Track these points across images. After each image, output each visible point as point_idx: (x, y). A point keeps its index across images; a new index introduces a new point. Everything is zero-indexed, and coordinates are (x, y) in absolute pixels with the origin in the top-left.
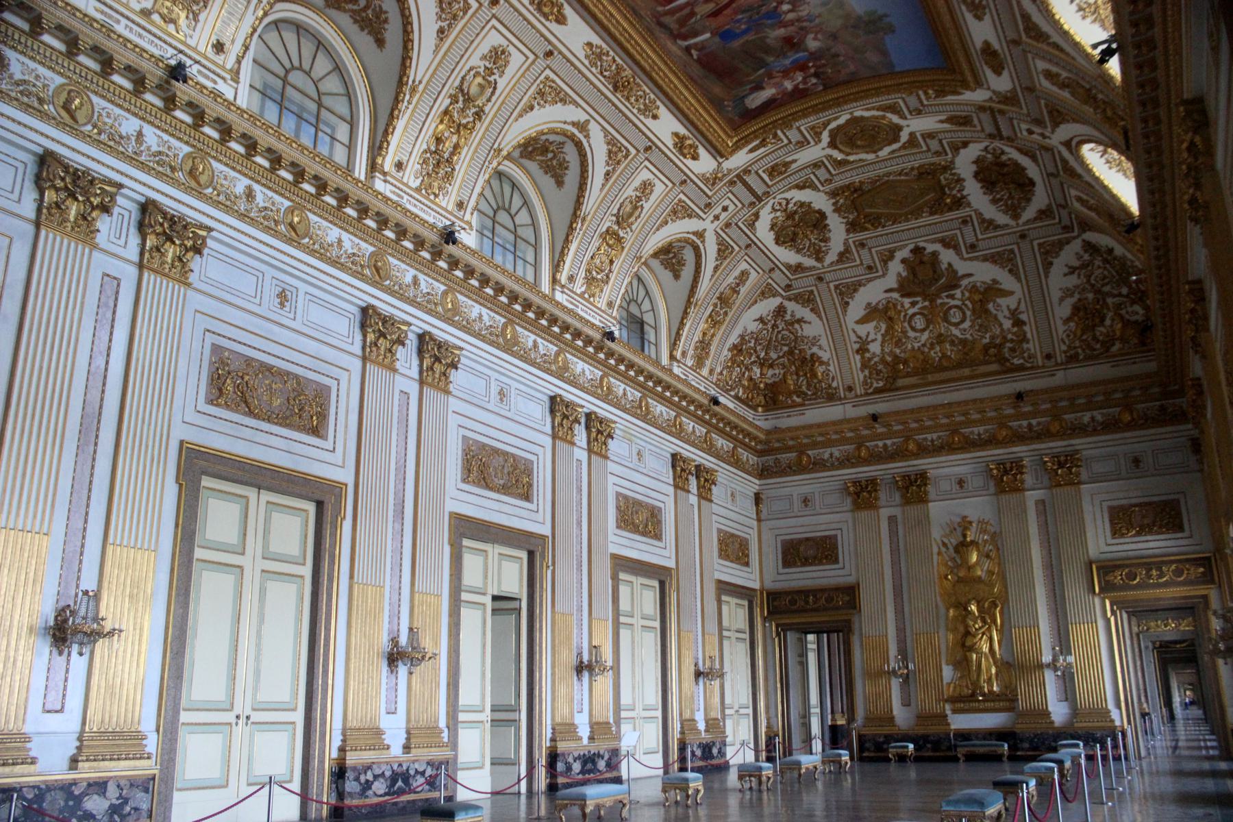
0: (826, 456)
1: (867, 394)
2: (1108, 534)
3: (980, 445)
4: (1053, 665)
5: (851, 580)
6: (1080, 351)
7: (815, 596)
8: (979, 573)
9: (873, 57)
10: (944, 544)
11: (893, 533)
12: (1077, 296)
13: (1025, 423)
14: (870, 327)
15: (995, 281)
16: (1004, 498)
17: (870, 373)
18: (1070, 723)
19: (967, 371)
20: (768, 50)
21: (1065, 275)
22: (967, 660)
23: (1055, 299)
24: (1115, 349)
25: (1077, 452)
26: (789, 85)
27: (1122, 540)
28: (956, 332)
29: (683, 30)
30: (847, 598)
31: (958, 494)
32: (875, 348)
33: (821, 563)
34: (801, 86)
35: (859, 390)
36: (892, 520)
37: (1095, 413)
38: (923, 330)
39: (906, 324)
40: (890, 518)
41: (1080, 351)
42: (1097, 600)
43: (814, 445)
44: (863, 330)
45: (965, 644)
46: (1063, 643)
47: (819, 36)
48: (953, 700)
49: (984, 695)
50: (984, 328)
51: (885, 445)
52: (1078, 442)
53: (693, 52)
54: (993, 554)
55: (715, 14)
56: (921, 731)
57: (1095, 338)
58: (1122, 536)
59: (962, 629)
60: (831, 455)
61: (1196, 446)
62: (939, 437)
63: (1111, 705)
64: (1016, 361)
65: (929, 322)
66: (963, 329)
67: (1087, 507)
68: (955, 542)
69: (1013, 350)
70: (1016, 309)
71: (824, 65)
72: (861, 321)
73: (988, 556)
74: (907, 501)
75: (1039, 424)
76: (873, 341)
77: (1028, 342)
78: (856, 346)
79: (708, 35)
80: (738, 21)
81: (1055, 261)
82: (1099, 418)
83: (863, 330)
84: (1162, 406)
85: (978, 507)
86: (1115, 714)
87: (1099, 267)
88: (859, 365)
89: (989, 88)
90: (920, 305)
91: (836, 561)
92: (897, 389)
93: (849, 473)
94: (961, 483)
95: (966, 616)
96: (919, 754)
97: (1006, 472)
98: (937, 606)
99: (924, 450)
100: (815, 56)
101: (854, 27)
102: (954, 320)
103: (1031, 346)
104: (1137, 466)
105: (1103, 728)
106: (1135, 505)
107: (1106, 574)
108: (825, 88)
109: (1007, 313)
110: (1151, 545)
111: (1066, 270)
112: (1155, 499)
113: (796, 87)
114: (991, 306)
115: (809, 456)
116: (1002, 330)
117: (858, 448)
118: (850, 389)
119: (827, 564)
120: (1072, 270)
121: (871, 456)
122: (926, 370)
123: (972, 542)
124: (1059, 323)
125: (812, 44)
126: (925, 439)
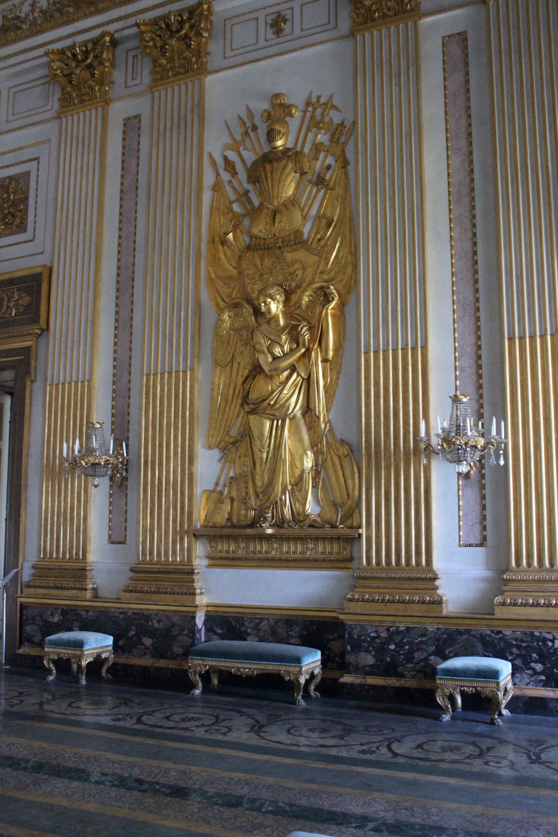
10: (229, 165)
11: (130, 152)
18: (484, 609)
30: (26, 300)
36: (132, 125)
48: (212, 534)
49: (280, 523)
68: (250, 157)
73: (320, 181)
74: (160, 77)
91: (22, 228)
93: (60, 36)
96: (123, 660)
98: (198, 306)
123: (287, 154)
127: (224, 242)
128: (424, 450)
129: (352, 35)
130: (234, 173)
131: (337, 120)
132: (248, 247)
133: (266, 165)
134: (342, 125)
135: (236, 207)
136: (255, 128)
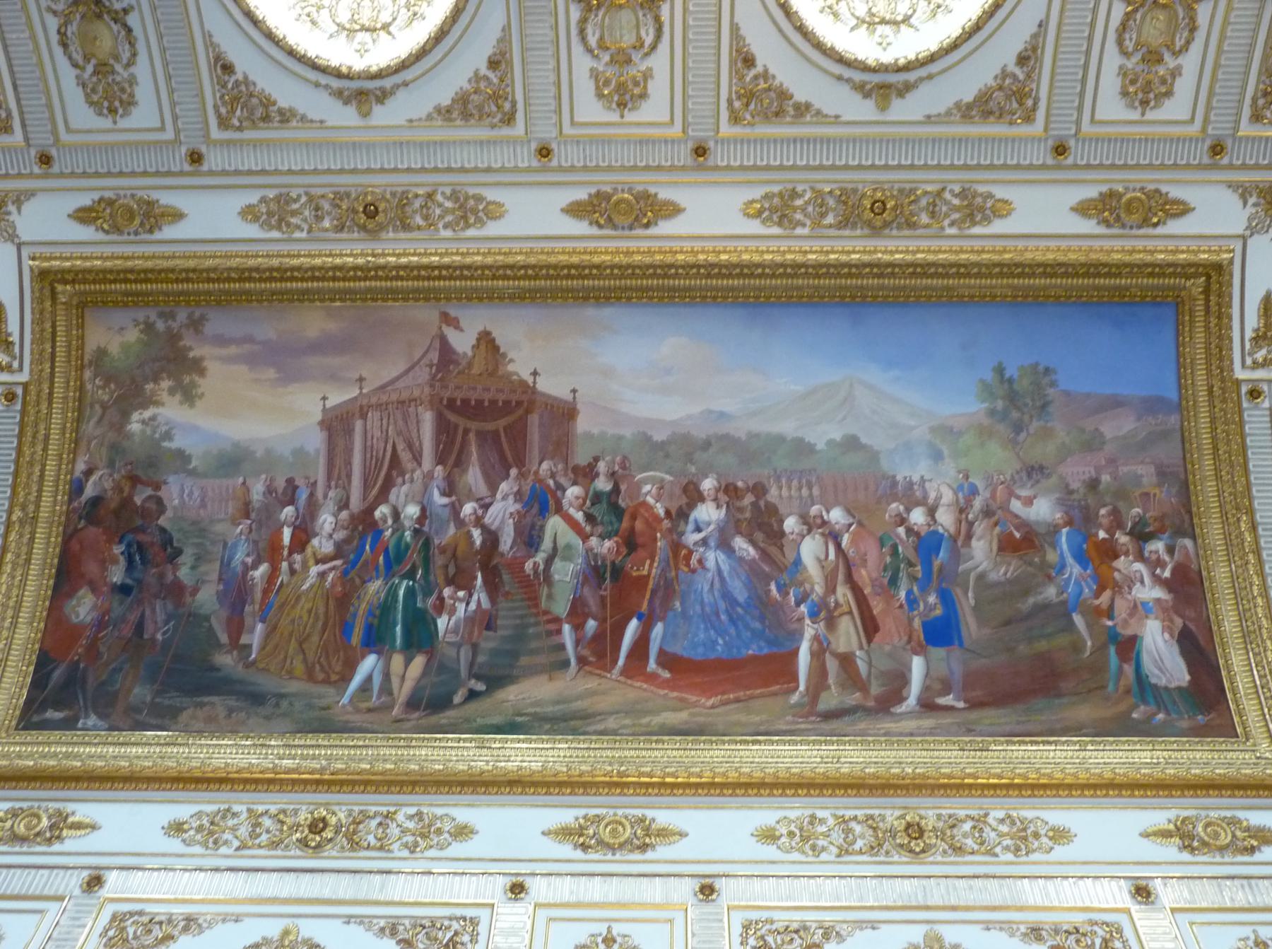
9: (1118, 427)
20: (1020, 587)
26: (1149, 592)
29: (875, 689)
34: (1167, 574)
47: (1024, 493)
53: (942, 701)
55: (870, 627)
71: (1115, 513)
79: (917, 666)
80: (912, 601)
89: (1244, 239)
100: (1080, 516)
101: (1018, 428)
108: (1194, 538)
113: (1158, 580)
125: (1043, 510)
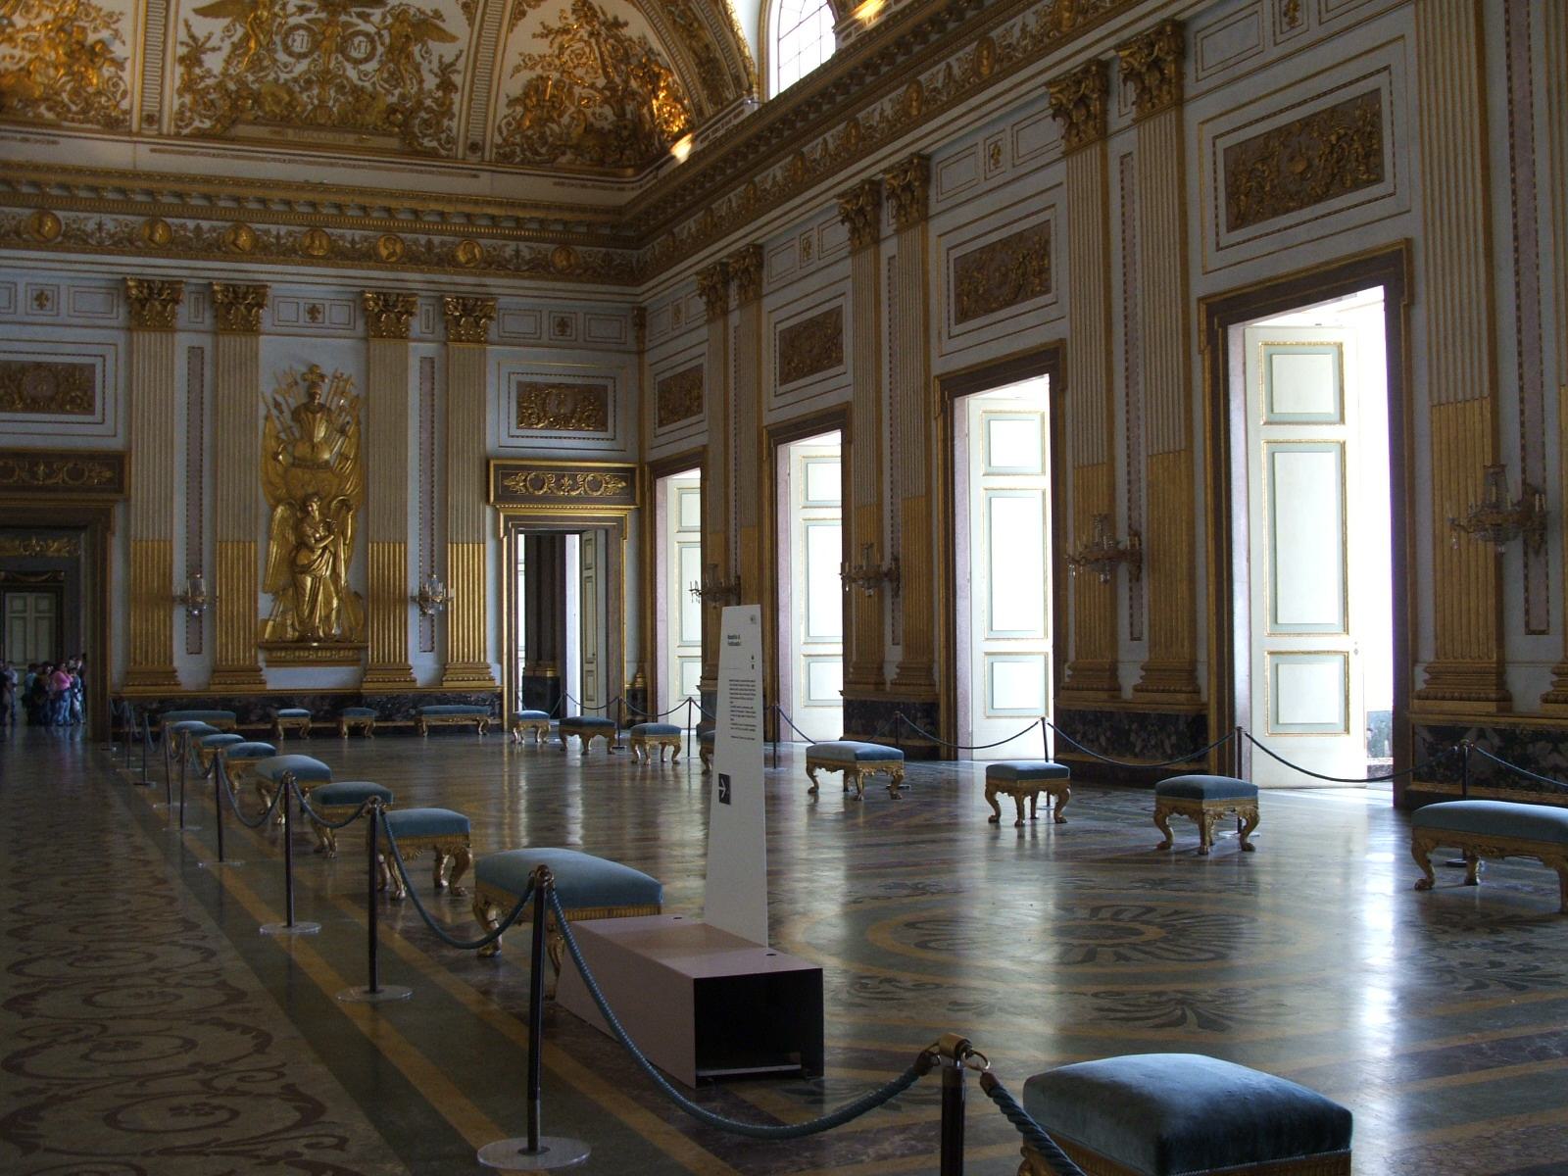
0: (91, 226)
1: (178, 136)
2: (514, 421)
3: (353, 259)
4: (423, 600)
5: (116, 444)
6: (518, 149)
7: (48, 465)
8: (326, 456)
10: (277, 405)
11: (195, 374)
12: (539, 71)
13: (423, 239)
14: (217, 25)
15: (437, 14)
16: (376, 343)
17: (195, 102)
19: (350, 139)
21: (534, 36)
22: (298, 587)
23: (508, 68)
24: (563, 160)
25: (493, 297)
27: (529, 432)
28: (352, 73)
30: (108, 474)
31: (306, 326)
32: (214, 62)
33: (61, 410)
35: (167, 126)
36: (196, 353)
37: (522, 245)
38: (304, 56)
39: (277, 39)
40: (191, 349)
41: (518, 149)
42: (489, 511)
43: (72, 203)
44: (203, 27)
45: (295, 567)
46: (438, 566)
48: (269, 647)
49: (319, 640)
50: (395, 79)
51: (198, 228)
52: (496, 284)
54: (351, 430)
56: (218, 690)
57: (542, 137)
58: (530, 426)
59: (292, 538)
60: (100, 226)
61: (640, 319)
62: (290, 234)
63: (491, 659)
64: (427, 143)
65: (316, 45)
66: (364, 72)
67: (491, 379)
68: (293, 403)
69: (425, 121)
70: (452, 64)
72: (203, 12)
73: (342, 431)
75: (443, 244)
76: (214, 49)
77: (451, 119)
78: (182, 51)
81: (530, 12)
82: (526, 253)
83: (203, 27)
84: (607, 254)
85: (336, 354)
86: (495, 671)
87: (581, 39)
88: (178, 83)
90: (311, 15)
91: (88, 407)
92: (233, 140)
93: (132, 264)
94: (313, 312)
95: (302, 520)
97: (387, 307)
99: (263, 250)
102: (354, 54)
103: (454, 124)
104: (563, 333)
105: (480, 690)
106: (553, 386)
107: (506, 476)
109: (435, 66)
110: (566, 443)
111: (539, 29)
112: (579, 381)
114: (416, 49)
115: (57, 220)
116: (421, 89)
117: (152, 225)
118: (150, 119)
119: (71, 412)
120: (547, 32)
121: (172, 241)
122: (282, 119)
123: (322, 407)
124: (503, 101)
126: (267, 232)
127: (275, 459)
128: (403, 600)
129: (366, 339)
130: (281, 412)
131: (354, 393)
132: (293, 465)
133: (306, 411)
134: (357, 396)
135: (282, 436)
136: (296, 383)
